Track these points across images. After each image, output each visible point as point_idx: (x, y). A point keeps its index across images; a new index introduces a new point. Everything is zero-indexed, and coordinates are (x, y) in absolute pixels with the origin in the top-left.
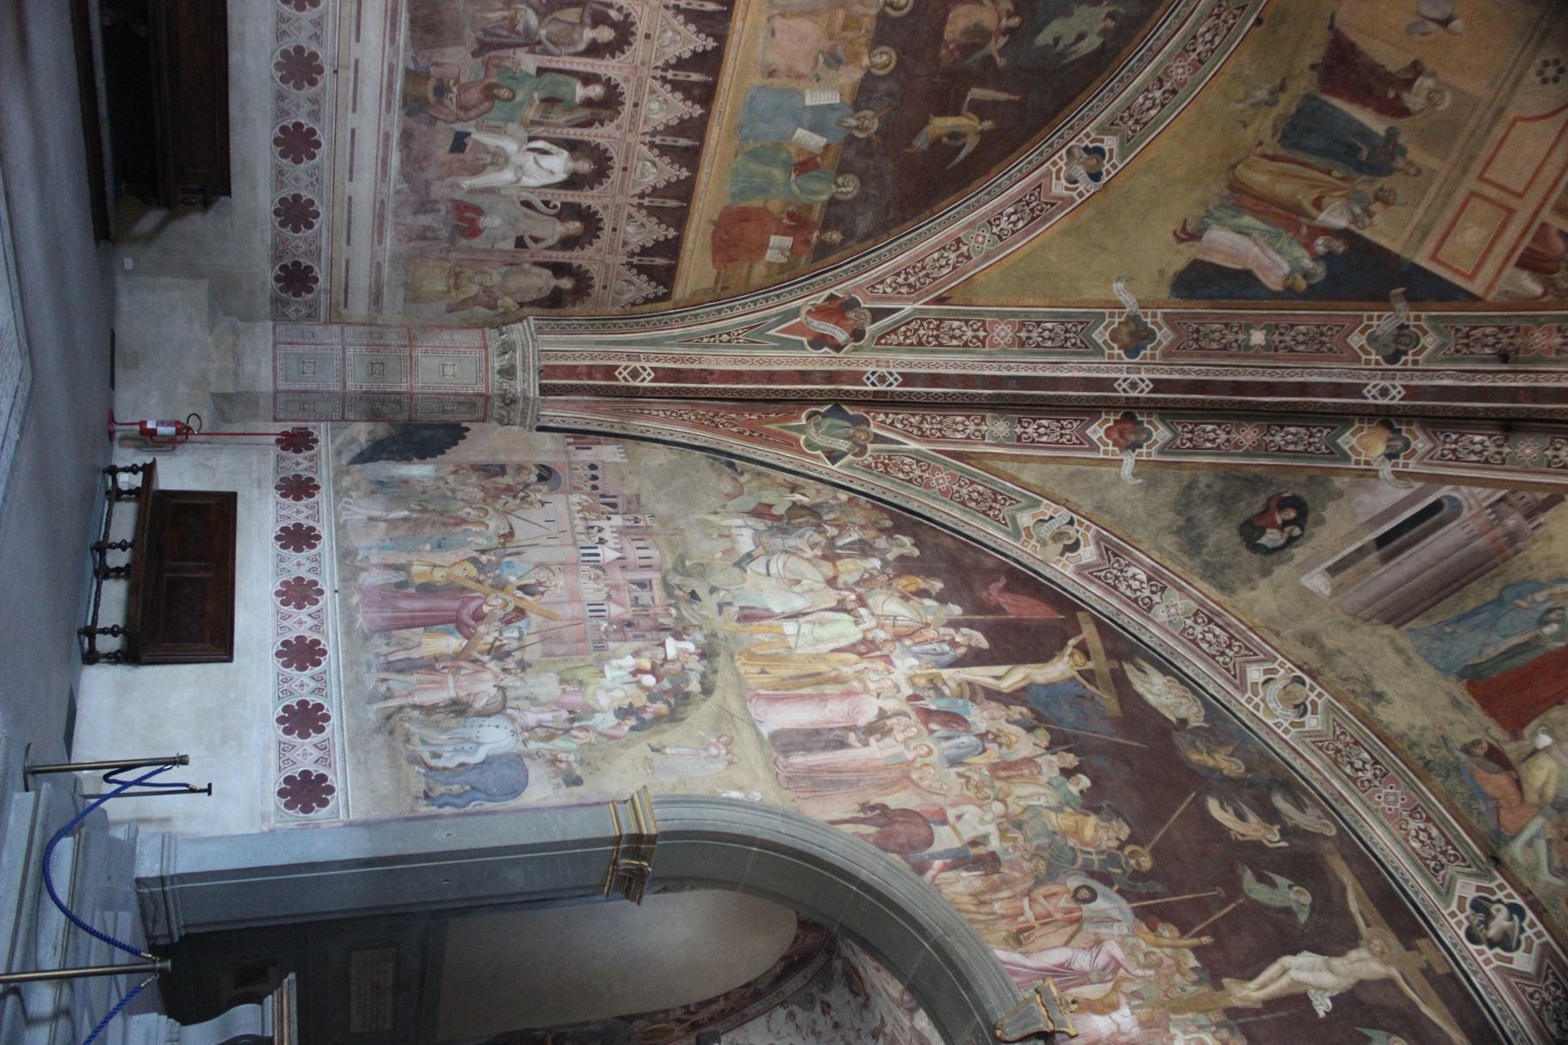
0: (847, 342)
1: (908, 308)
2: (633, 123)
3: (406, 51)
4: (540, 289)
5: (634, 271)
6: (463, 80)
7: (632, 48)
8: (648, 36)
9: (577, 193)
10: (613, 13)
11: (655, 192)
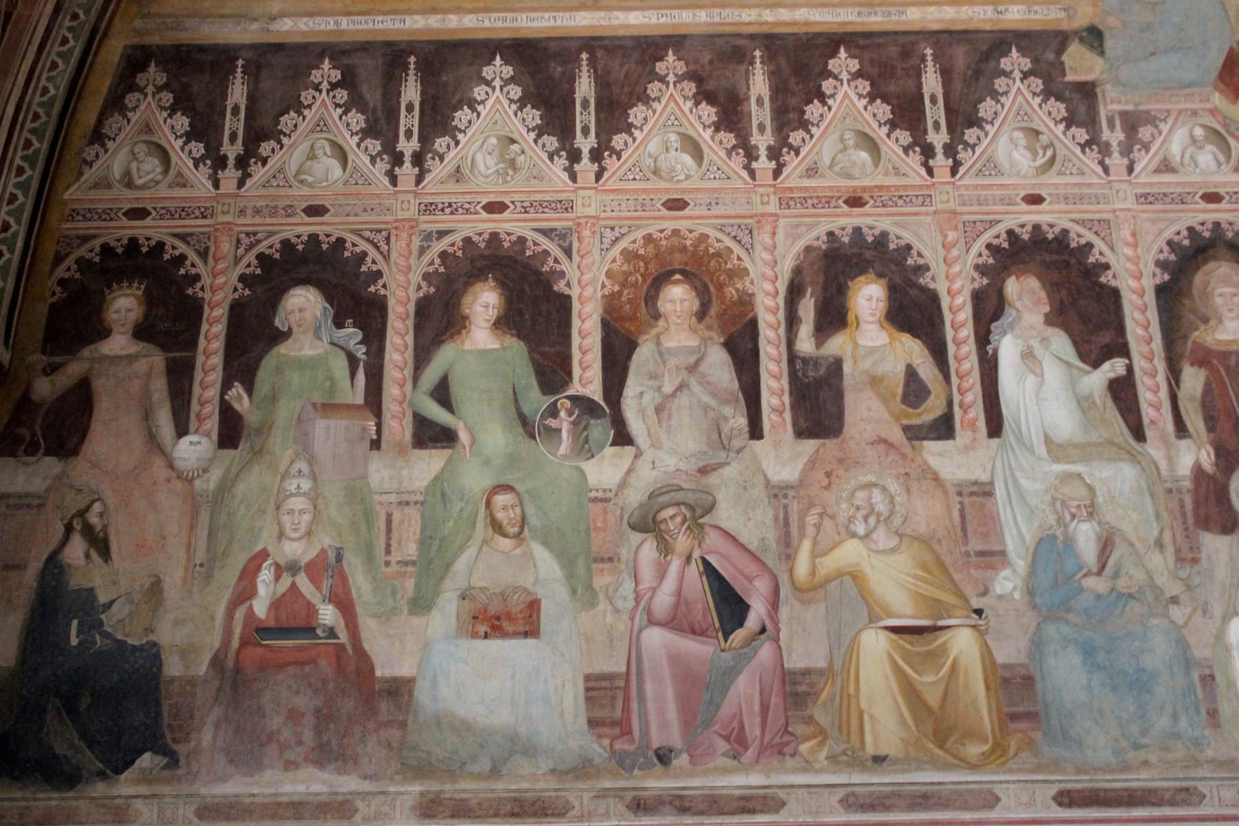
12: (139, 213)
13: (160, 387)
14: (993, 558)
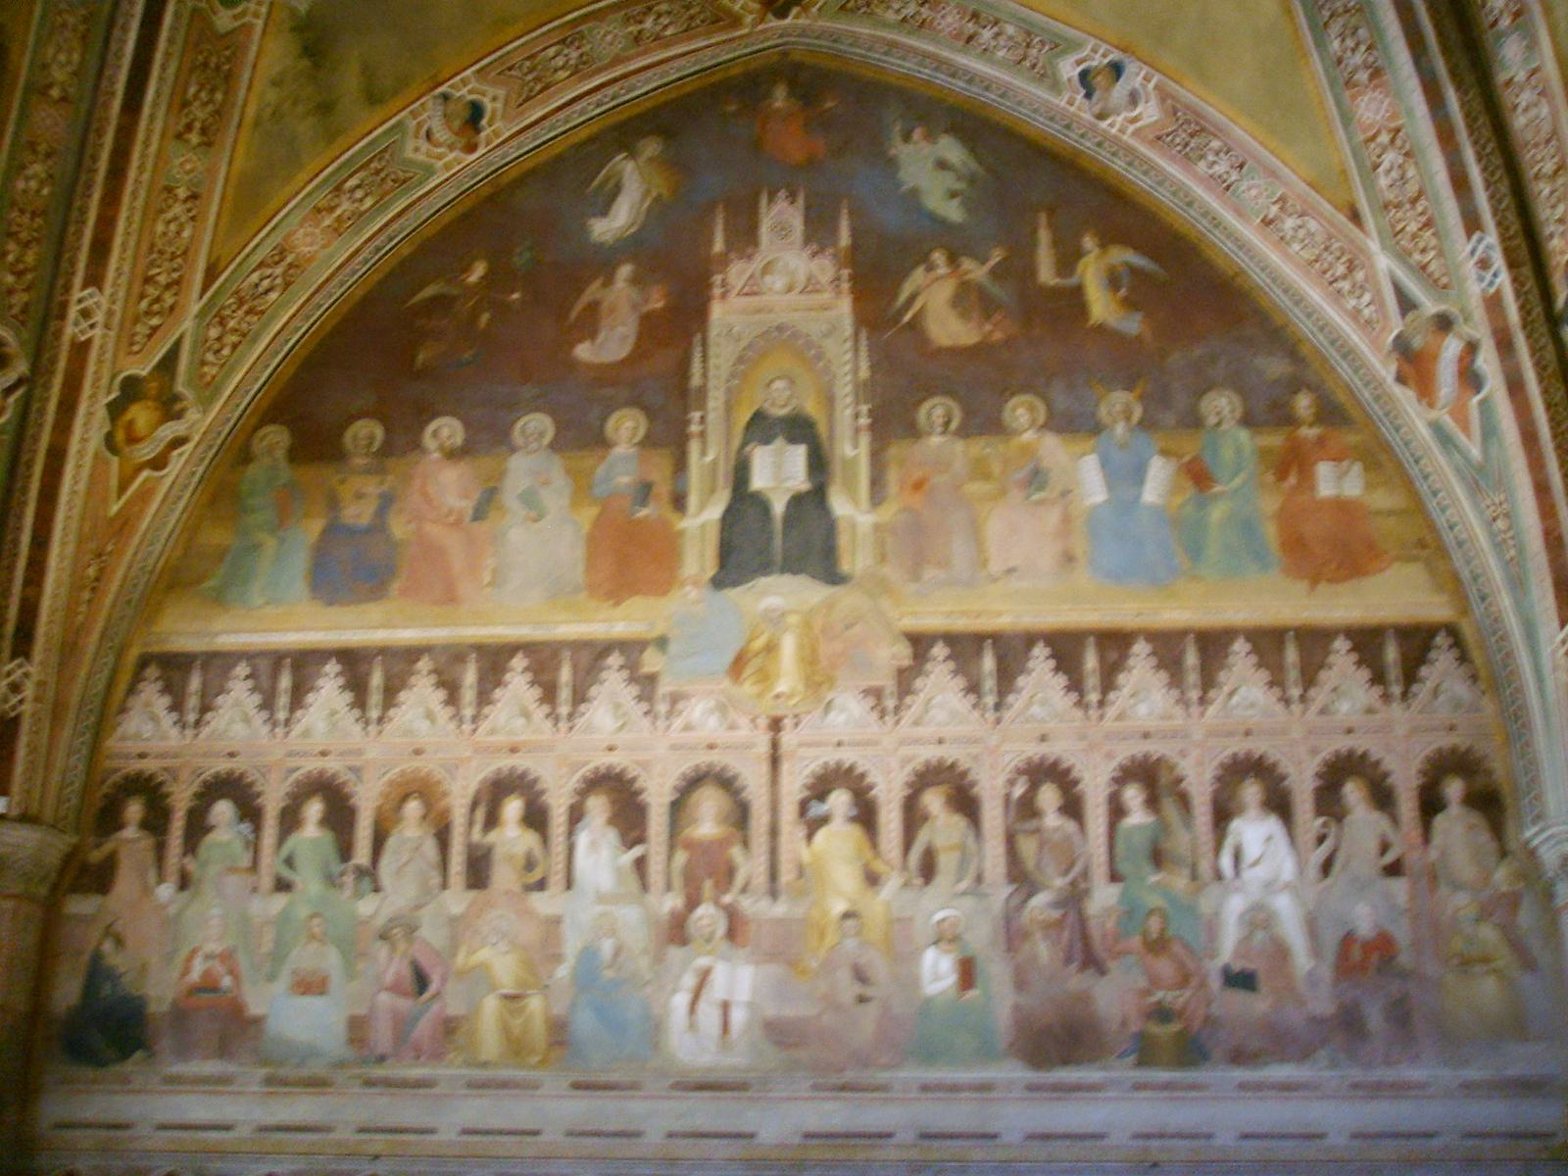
0: (1460, 336)
1: (1383, 263)
2: (1174, 734)
4: (1471, 828)
8: (1043, 738)
10: (1019, 791)
11: (1277, 682)
12: (142, 756)
13: (150, 857)
14: (557, 958)
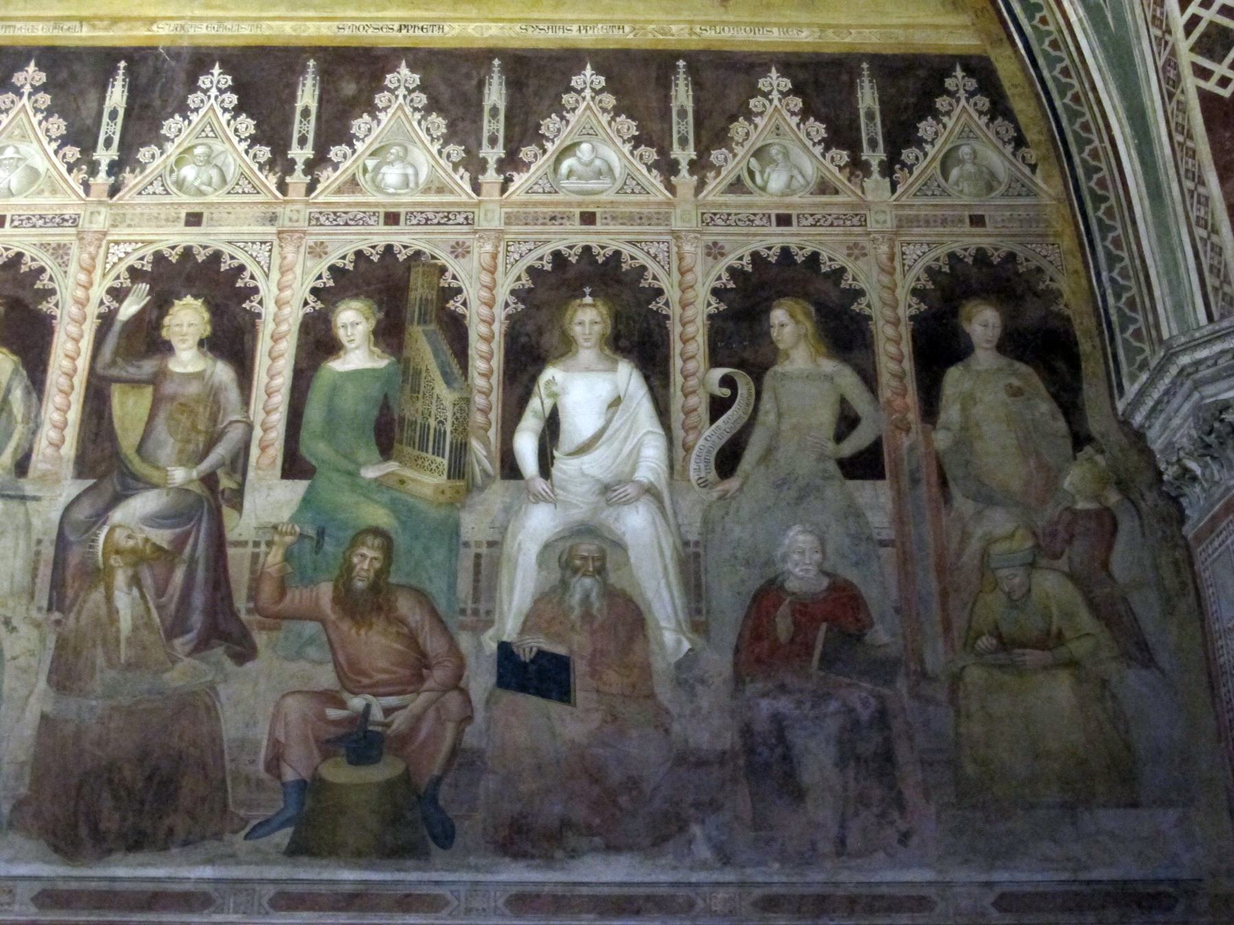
3: (232, 858)
4: (1016, 393)
5: (908, 154)
6: (326, 678)
7: (227, 250)
8: (194, 219)
9: (676, 330)
10: (129, 309)
